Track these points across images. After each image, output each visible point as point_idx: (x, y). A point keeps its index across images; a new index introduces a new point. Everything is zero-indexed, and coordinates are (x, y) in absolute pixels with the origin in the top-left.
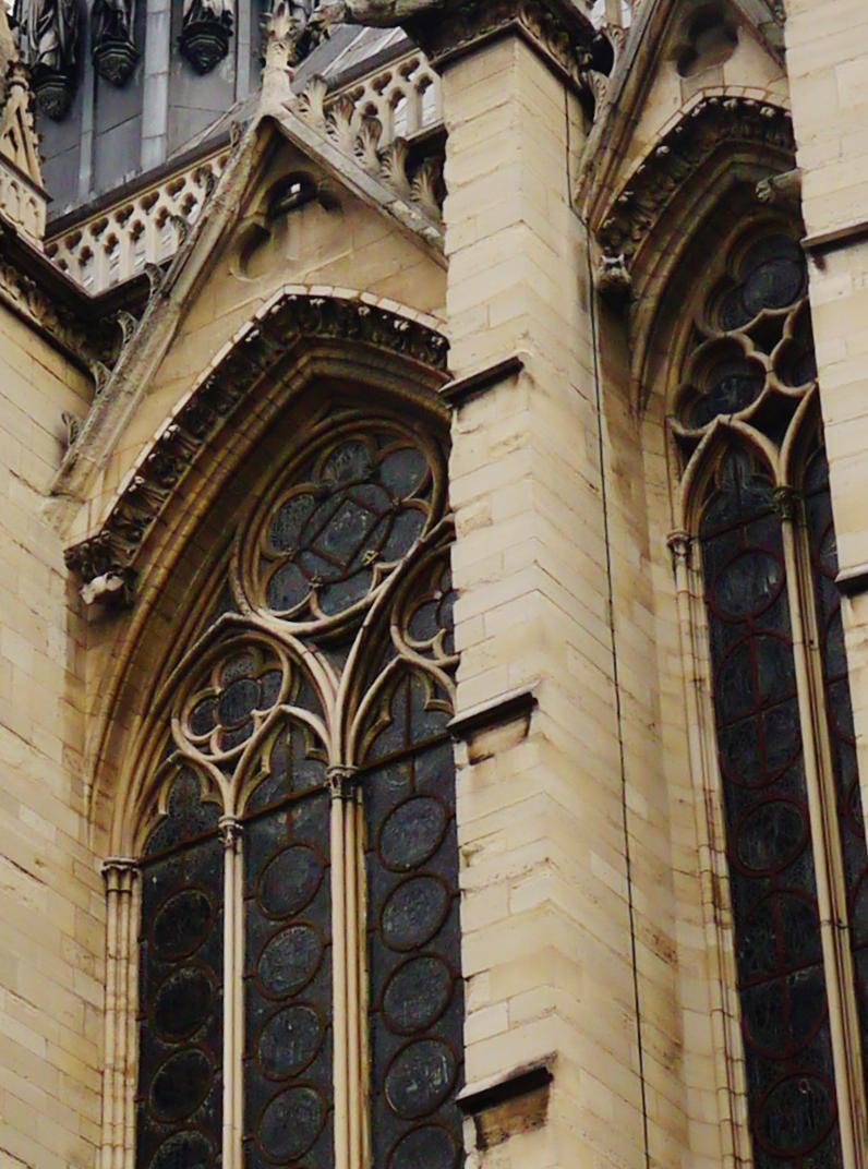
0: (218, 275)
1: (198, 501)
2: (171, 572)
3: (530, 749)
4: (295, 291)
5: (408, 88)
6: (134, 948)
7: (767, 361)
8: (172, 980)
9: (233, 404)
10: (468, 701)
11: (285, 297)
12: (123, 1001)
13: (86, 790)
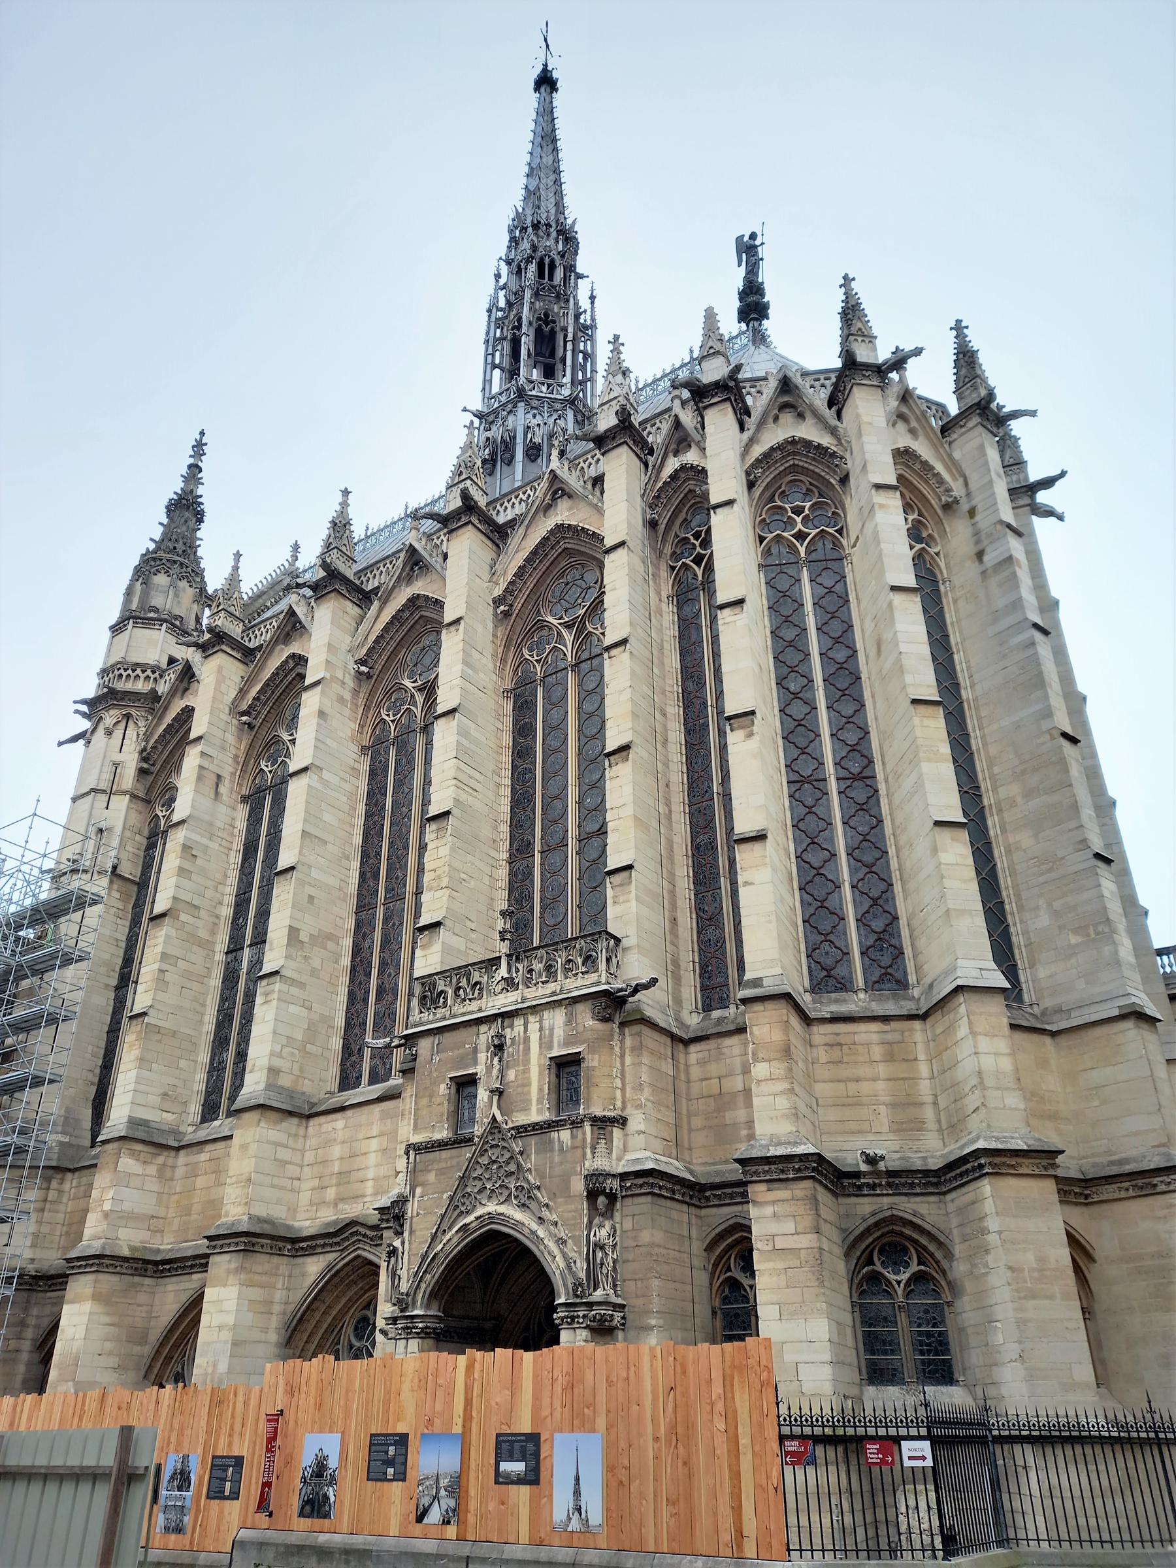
1: (531, 584)
3: (626, 655)
4: (559, 522)
5: (593, 462)
7: (697, 543)
10: (607, 641)
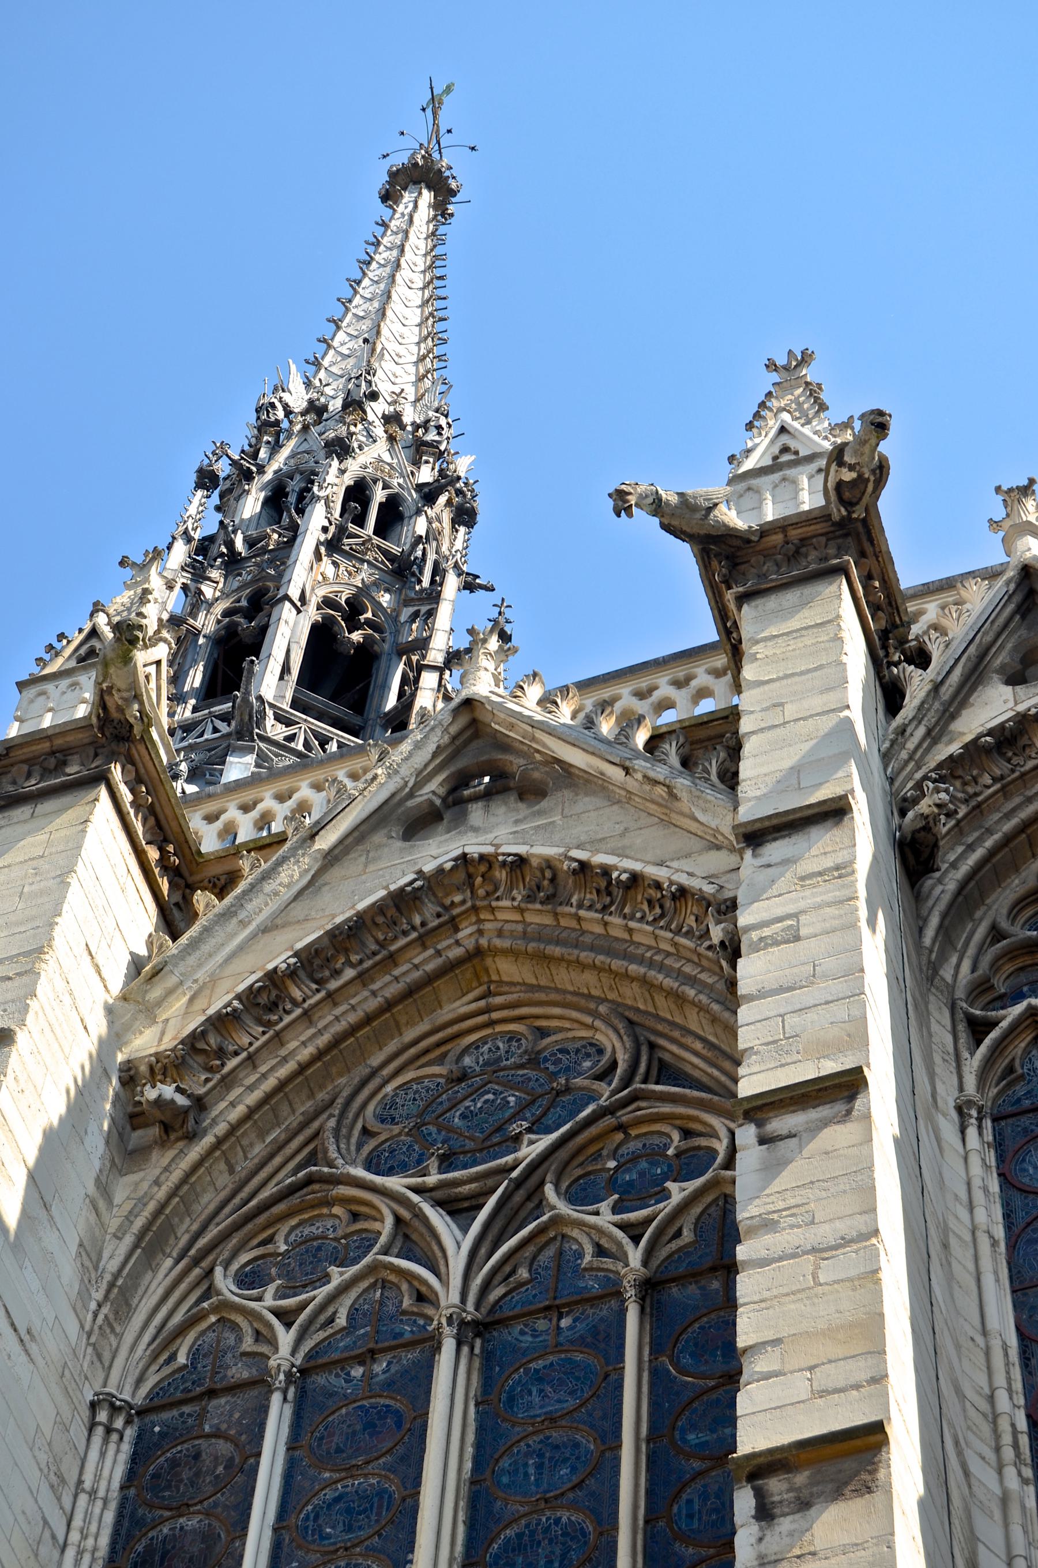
0: (379, 838)
1: (301, 1047)
2: (252, 1111)
6: (115, 1494)
8: (165, 1531)
9: (369, 958)
11: (464, 855)
12: (90, 1542)
13: (93, 1306)
